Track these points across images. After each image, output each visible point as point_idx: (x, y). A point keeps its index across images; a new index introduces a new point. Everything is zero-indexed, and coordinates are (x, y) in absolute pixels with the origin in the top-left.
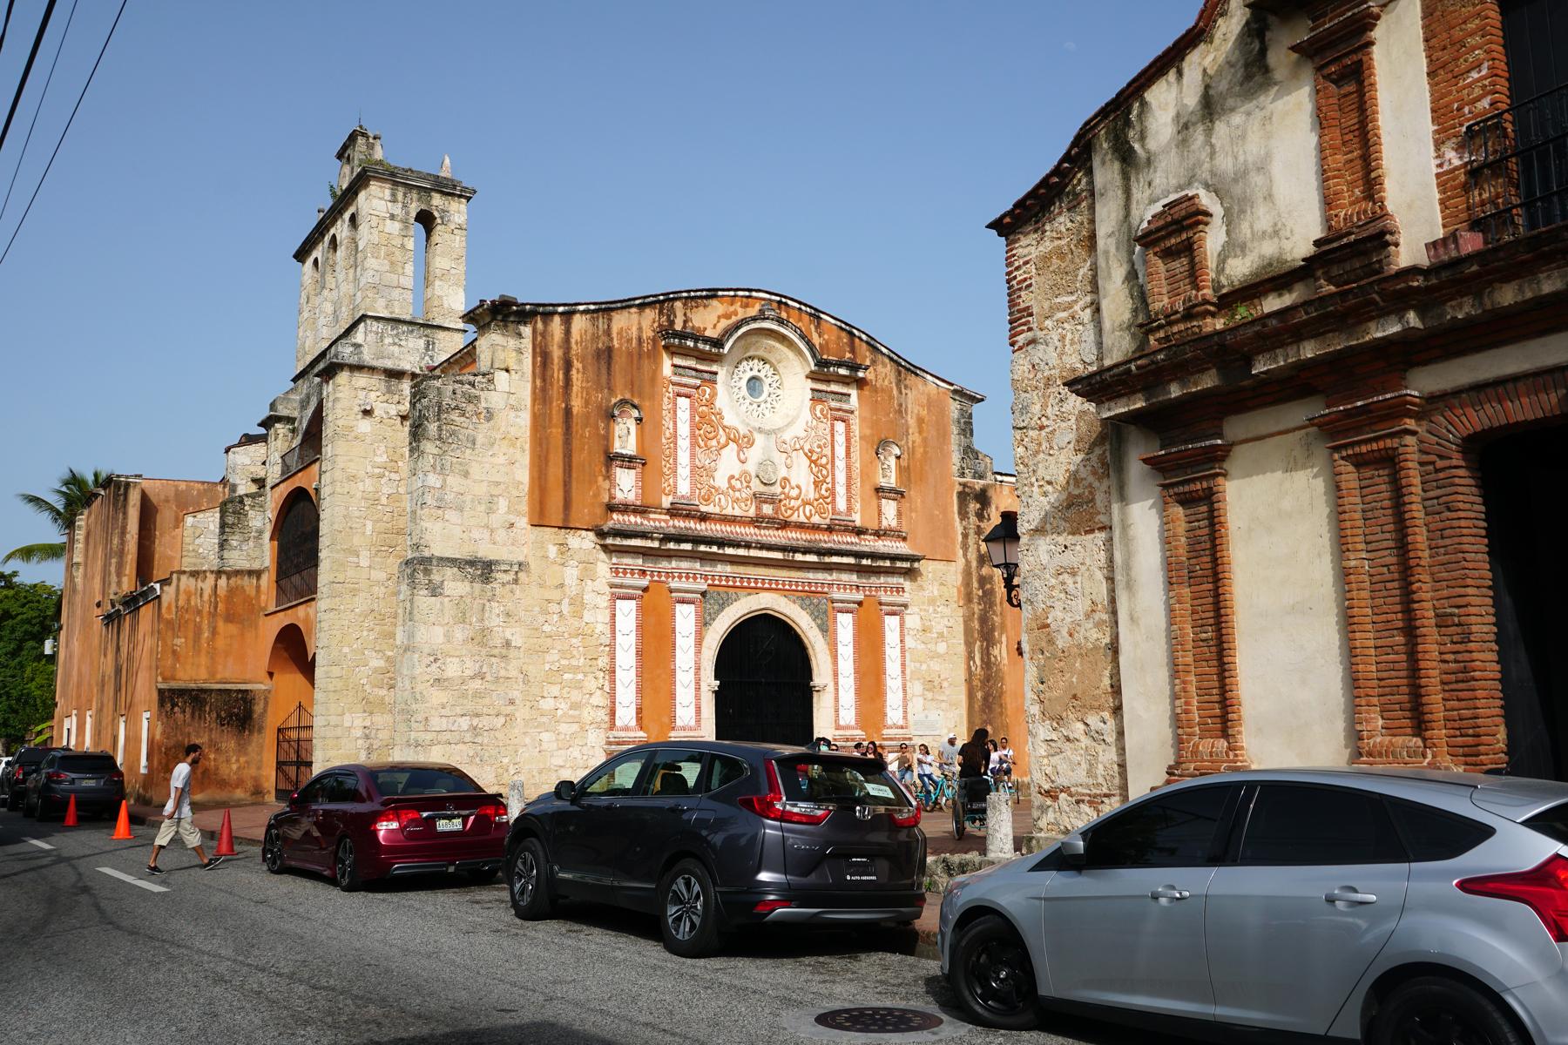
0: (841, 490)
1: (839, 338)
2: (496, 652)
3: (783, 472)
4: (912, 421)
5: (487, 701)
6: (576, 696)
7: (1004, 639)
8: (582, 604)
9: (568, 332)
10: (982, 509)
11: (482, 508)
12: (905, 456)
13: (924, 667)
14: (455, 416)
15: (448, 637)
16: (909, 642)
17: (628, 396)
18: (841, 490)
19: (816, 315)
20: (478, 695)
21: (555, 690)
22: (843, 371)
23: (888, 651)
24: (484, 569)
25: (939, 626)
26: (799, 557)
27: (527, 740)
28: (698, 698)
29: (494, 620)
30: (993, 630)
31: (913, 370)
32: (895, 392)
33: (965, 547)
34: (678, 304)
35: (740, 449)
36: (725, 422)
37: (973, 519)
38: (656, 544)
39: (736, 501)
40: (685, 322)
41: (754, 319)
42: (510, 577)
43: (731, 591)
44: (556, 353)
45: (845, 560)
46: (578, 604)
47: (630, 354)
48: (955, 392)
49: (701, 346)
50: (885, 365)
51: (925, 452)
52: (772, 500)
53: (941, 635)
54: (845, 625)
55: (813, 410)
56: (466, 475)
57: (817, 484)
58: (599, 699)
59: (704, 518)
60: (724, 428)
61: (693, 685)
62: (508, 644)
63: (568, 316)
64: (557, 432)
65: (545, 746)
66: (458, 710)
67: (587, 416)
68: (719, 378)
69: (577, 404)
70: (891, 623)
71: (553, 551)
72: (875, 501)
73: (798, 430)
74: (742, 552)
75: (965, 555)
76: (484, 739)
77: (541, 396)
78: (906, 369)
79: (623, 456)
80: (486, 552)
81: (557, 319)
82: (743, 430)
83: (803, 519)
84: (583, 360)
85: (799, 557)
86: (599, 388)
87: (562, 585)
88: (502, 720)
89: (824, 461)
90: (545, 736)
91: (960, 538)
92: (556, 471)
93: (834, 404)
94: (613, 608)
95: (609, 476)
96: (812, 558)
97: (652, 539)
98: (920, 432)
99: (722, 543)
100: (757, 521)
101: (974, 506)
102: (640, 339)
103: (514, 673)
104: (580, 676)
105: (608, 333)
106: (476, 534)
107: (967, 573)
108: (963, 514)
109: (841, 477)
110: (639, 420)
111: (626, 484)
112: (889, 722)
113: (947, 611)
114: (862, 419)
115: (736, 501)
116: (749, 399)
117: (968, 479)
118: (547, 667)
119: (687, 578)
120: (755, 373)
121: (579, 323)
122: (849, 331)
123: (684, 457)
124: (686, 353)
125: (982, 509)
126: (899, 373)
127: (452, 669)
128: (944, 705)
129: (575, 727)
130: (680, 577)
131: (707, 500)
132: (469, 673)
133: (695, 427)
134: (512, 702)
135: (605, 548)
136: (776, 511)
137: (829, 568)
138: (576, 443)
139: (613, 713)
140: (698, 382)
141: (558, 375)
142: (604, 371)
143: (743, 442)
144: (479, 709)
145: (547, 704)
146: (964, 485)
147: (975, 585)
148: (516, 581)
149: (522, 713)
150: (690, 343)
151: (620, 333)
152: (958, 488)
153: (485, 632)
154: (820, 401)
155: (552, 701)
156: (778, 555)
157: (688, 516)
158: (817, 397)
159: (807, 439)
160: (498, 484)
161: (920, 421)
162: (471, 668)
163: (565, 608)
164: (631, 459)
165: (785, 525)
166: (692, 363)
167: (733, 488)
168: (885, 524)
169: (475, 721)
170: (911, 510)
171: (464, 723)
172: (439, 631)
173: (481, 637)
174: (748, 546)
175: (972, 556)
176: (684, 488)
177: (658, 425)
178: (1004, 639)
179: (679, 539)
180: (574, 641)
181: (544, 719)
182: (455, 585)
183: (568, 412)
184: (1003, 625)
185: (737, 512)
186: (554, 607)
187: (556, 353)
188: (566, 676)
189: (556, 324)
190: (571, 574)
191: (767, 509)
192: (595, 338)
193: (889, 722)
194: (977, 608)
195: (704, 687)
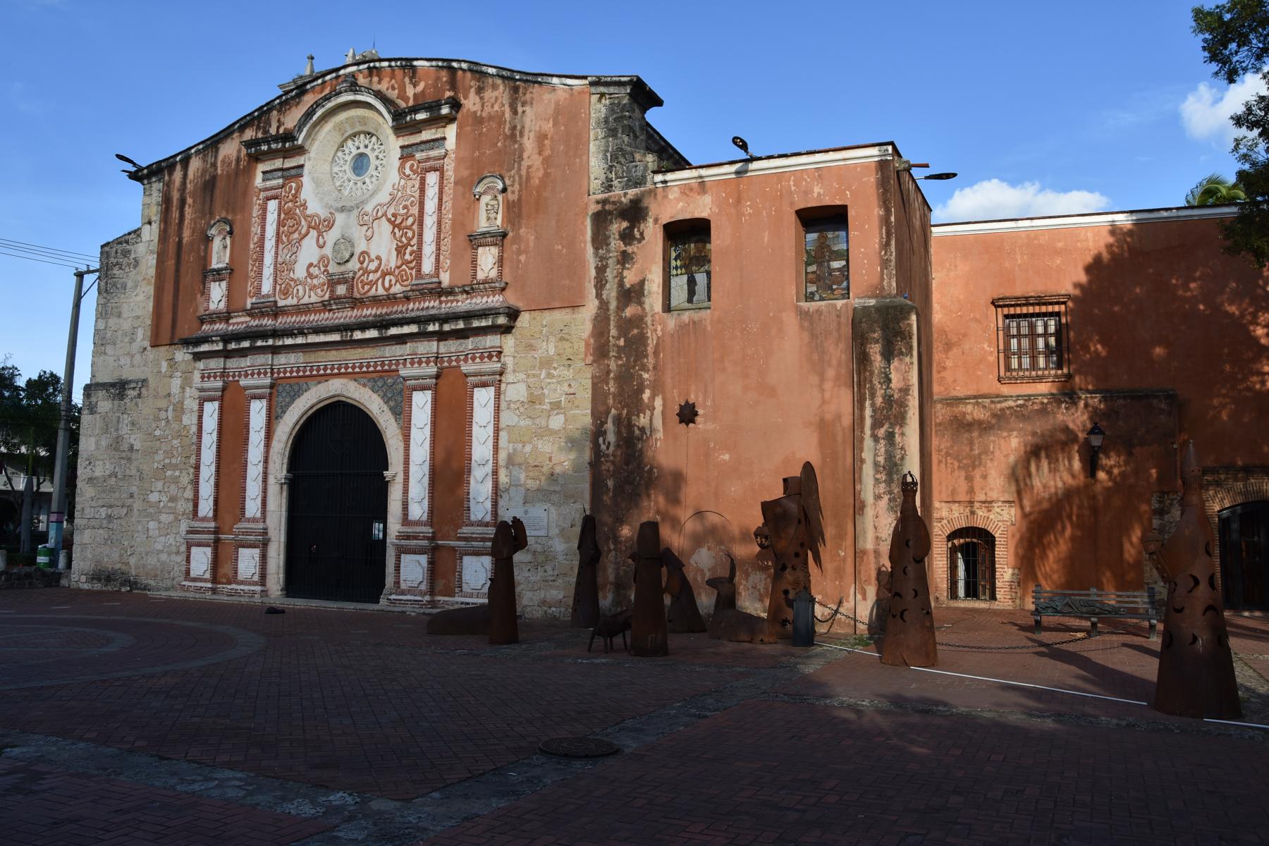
0: (429, 250)
1: (438, 79)
2: (124, 455)
3: (361, 246)
4: (529, 143)
5: (117, 495)
6: (173, 490)
7: (658, 403)
8: (182, 408)
9: (185, 176)
10: (631, 228)
11: (127, 340)
12: (517, 186)
13: (528, 448)
14: (116, 271)
15: (97, 443)
16: (507, 418)
17: (224, 215)
18: (429, 250)
19: (408, 65)
20: (112, 490)
21: (159, 485)
22: (421, 116)
23: (476, 430)
24: (119, 388)
25: (554, 392)
26: (358, 335)
27: (140, 528)
28: (265, 491)
29: (124, 430)
30: (640, 391)
31: (534, 79)
32: (508, 115)
33: (600, 284)
34: (275, 113)
35: (320, 234)
36: (309, 212)
37: (616, 244)
38: (220, 347)
39: (313, 288)
40: (278, 128)
41: (327, 99)
42: (135, 393)
43: (302, 381)
44: (176, 196)
45: (406, 330)
46: (180, 409)
47: (228, 176)
48: (591, 84)
49: (274, 146)
50: (495, 87)
51: (547, 175)
52: (343, 281)
53: (556, 406)
54: (422, 404)
55: (401, 169)
56: (119, 315)
57: (400, 250)
58: (189, 494)
59: (276, 312)
60: (306, 217)
61: (260, 478)
62: (131, 448)
63: (186, 162)
64: (171, 263)
65: (151, 533)
66: (101, 502)
67: (192, 243)
68: (306, 171)
69: (187, 234)
70: (483, 399)
71: (164, 365)
72: (468, 255)
73: (383, 197)
74: (300, 340)
75: (599, 296)
76: (114, 525)
77: (163, 237)
78: (520, 83)
79: (214, 270)
80: (128, 374)
81: (178, 167)
82: (323, 214)
83: (381, 291)
84: (193, 195)
85: (358, 335)
86: (203, 215)
87: (169, 395)
88: (125, 510)
89: (410, 220)
90: (152, 525)
91: (593, 273)
92: (168, 298)
93: (418, 156)
94: (201, 410)
95: (205, 292)
96: (373, 333)
97: (216, 342)
98: (540, 153)
99: (275, 334)
100: (325, 306)
101: (617, 226)
102: (238, 160)
103: (133, 472)
104: (177, 473)
105: (214, 165)
106: (122, 362)
107: (601, 321)
108: (600, 240)
109: (429, 235)
110: (231, 233)
111: (217, 294)
112: (473, 518)
113: (568, 374)
114: (459, 161)
115: (313, 288)
116: (354, 177)
117: (617, 192)
118: (156, 465)
119: (259, 374)
120: (362, 150)
121: (195, 164)
122: (447, 66)
123: (268, 258)
124: (271, 154)
125: (631, 228)
126: (516, 90)
127: (98, 473)
128: (555, 498)
129: (172, 517)
130: (252, 375)
131: (286, 293)
132: (108, 472)
133: (280, 224)
134: (132, 496)
135: (198, 357)
136: (351, 289)
137: (401, 339)
138: (183, 269)
139: (196, 505)
140: (281, 181)
141: (175, 214)
142: (208, 199)
143: (322, 226)
144: (112, 501)
145: (154, 497)
146: (604, 202)
147: (613, 332)
148: (139, 396)
149: (137, 505)
150: (264, 148)
151: (223, 161)
152: (594, 208)
153: (118, 439)
154: (412, 156)
155: (156, 494)
156: (336, 337)
157: (263, 315)
158: (407, 153)
159: (390, 203)
160: (138, 317)
161: (541, 138)
162: (109, 468)
163: (170, 414)
164: (218, 271)
165: (356, 303)
166: (278, 163)
167: (310, 275)
168: (481, 276)
169: (110, 511)
170: (519, 252)
171: (103, 512)
172: (93, 440)
173: (116, 444)
174: (301, 332)
175: (611, 292)
176: (267, 287)
177: (247, 234)
178: (658, 403)
179: (238, 337)
180: (175, 442)
181: (151, 510)
182: (104, 404)
183: (180, 243)
184: (657, 388)
185: (314, 299)
186: (163, 415)
187: (176, 196)
188: (169, 473)
189: (178, 175)
190: (176, 383)
191: (341, 290)
192: (204, 171)
193: (473, 518)
194: (613, 365)
195: (271, 480)
